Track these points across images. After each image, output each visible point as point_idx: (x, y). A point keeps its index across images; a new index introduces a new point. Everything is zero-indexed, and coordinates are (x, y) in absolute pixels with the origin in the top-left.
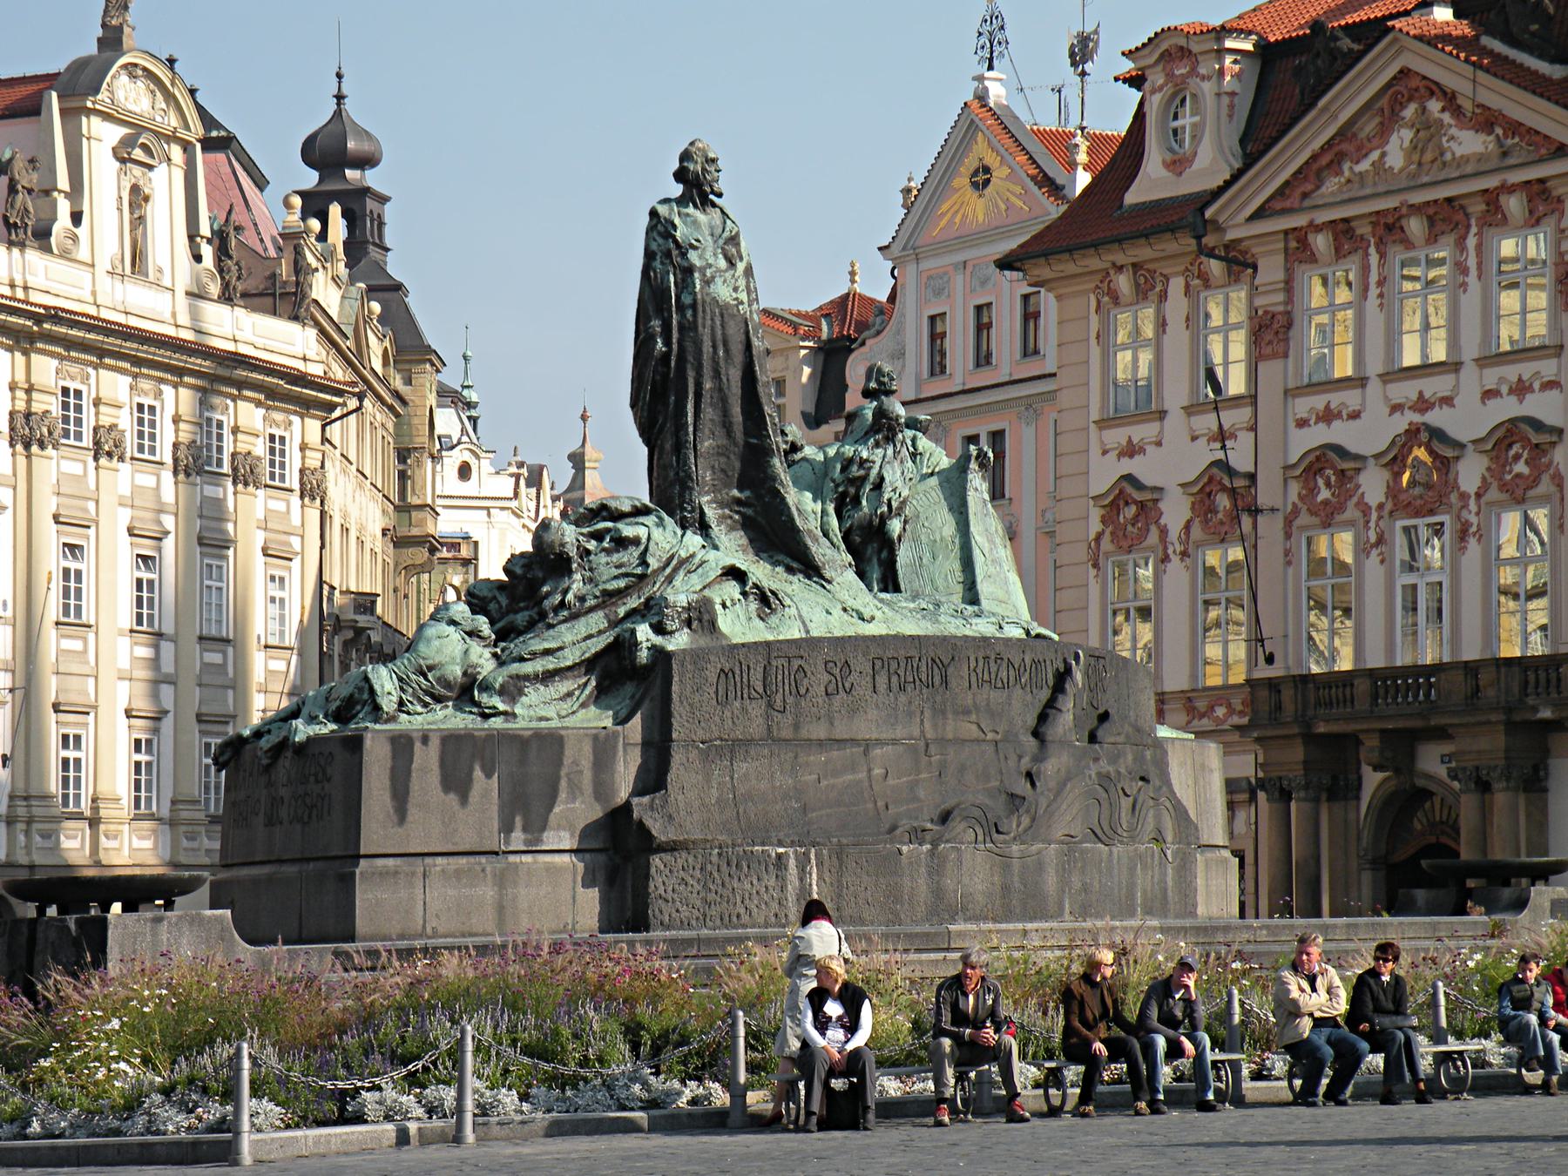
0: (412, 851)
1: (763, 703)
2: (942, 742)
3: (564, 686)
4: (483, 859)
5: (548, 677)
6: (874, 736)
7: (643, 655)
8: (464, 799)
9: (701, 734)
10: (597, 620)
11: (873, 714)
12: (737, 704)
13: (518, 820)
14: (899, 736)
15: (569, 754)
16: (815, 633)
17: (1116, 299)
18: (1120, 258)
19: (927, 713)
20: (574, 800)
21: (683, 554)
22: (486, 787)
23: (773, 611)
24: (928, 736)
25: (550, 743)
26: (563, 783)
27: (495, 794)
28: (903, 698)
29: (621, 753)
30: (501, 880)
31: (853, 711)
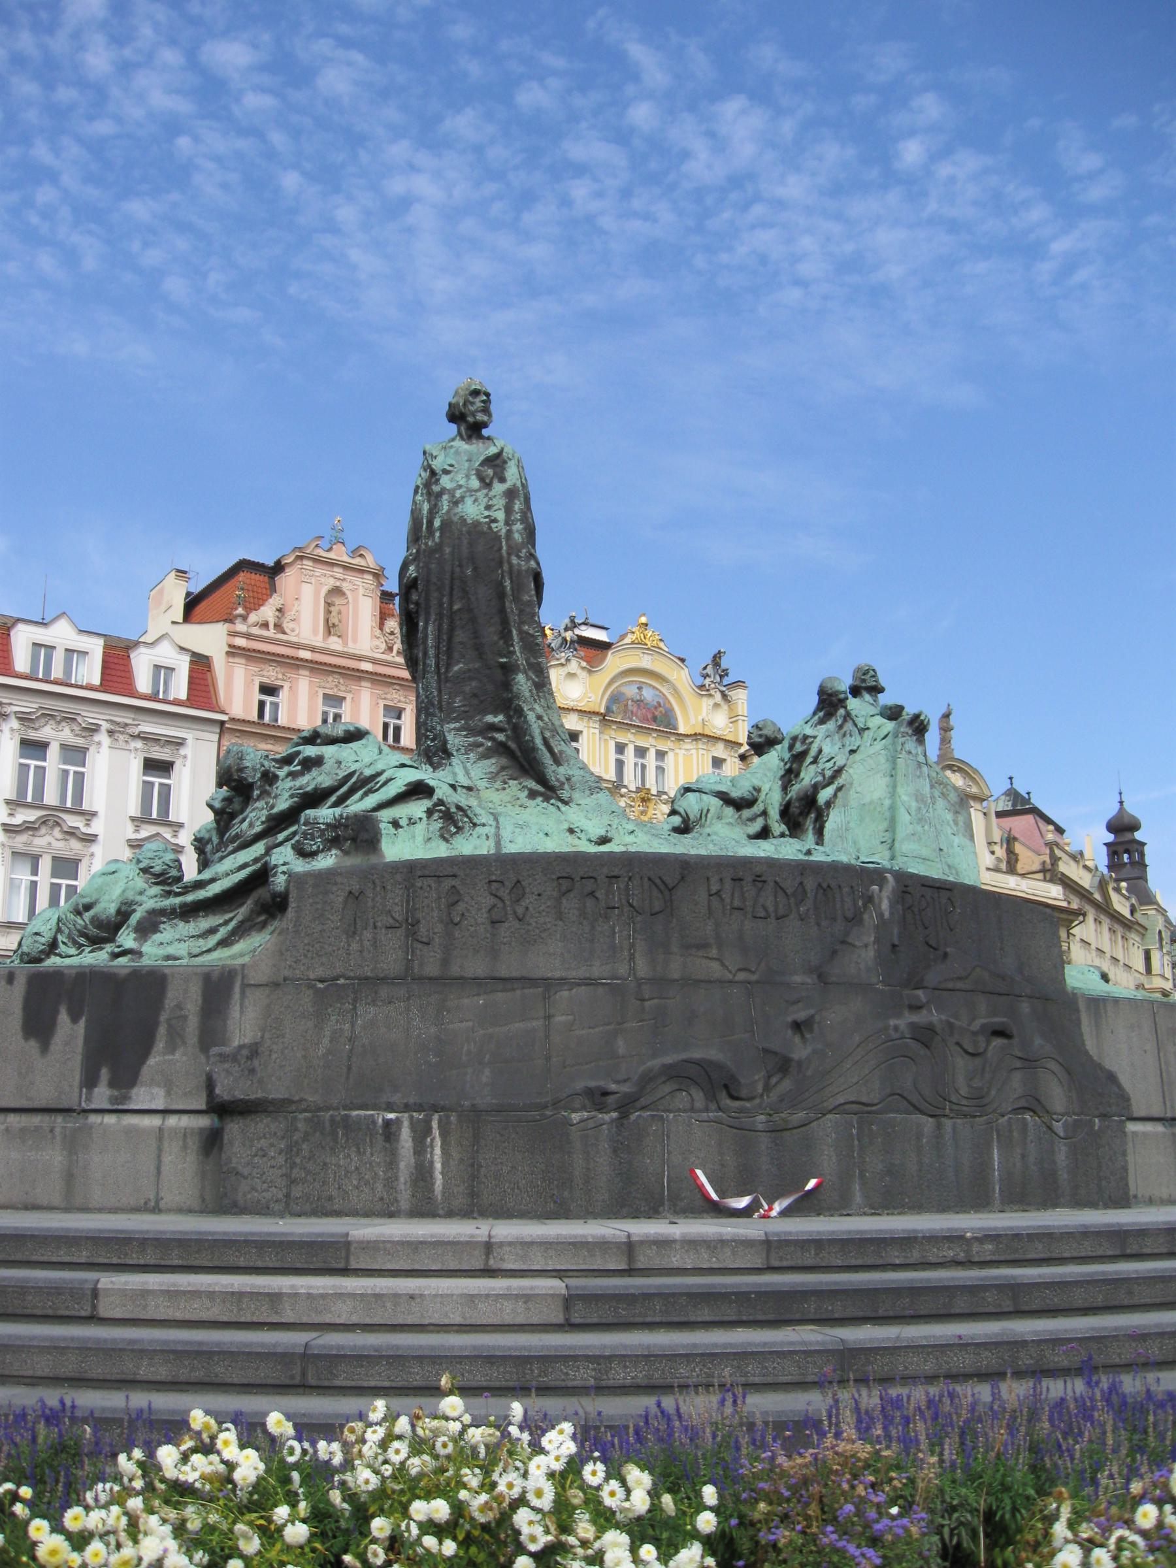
1: (401, 932)
3: (205, 923)
4: (59, 1119)
5: (189, 912)
6: (557, 974)
7: (279, 881)
8: (45, 1047)
9: (320, 972)
10: (259, 848)
12: (368, 934)
13: (105, 1073)
14: (596, 974)
15: (172, 996)
16: (504, 851)
19: (641, 946)
20: (173, 1052)
21: (368, 772)
22: (70, 1033)
23: (459, 829)
25: (151, 984)
26: (162, 1030)
27: (80, 1041)
29: (237, 996)
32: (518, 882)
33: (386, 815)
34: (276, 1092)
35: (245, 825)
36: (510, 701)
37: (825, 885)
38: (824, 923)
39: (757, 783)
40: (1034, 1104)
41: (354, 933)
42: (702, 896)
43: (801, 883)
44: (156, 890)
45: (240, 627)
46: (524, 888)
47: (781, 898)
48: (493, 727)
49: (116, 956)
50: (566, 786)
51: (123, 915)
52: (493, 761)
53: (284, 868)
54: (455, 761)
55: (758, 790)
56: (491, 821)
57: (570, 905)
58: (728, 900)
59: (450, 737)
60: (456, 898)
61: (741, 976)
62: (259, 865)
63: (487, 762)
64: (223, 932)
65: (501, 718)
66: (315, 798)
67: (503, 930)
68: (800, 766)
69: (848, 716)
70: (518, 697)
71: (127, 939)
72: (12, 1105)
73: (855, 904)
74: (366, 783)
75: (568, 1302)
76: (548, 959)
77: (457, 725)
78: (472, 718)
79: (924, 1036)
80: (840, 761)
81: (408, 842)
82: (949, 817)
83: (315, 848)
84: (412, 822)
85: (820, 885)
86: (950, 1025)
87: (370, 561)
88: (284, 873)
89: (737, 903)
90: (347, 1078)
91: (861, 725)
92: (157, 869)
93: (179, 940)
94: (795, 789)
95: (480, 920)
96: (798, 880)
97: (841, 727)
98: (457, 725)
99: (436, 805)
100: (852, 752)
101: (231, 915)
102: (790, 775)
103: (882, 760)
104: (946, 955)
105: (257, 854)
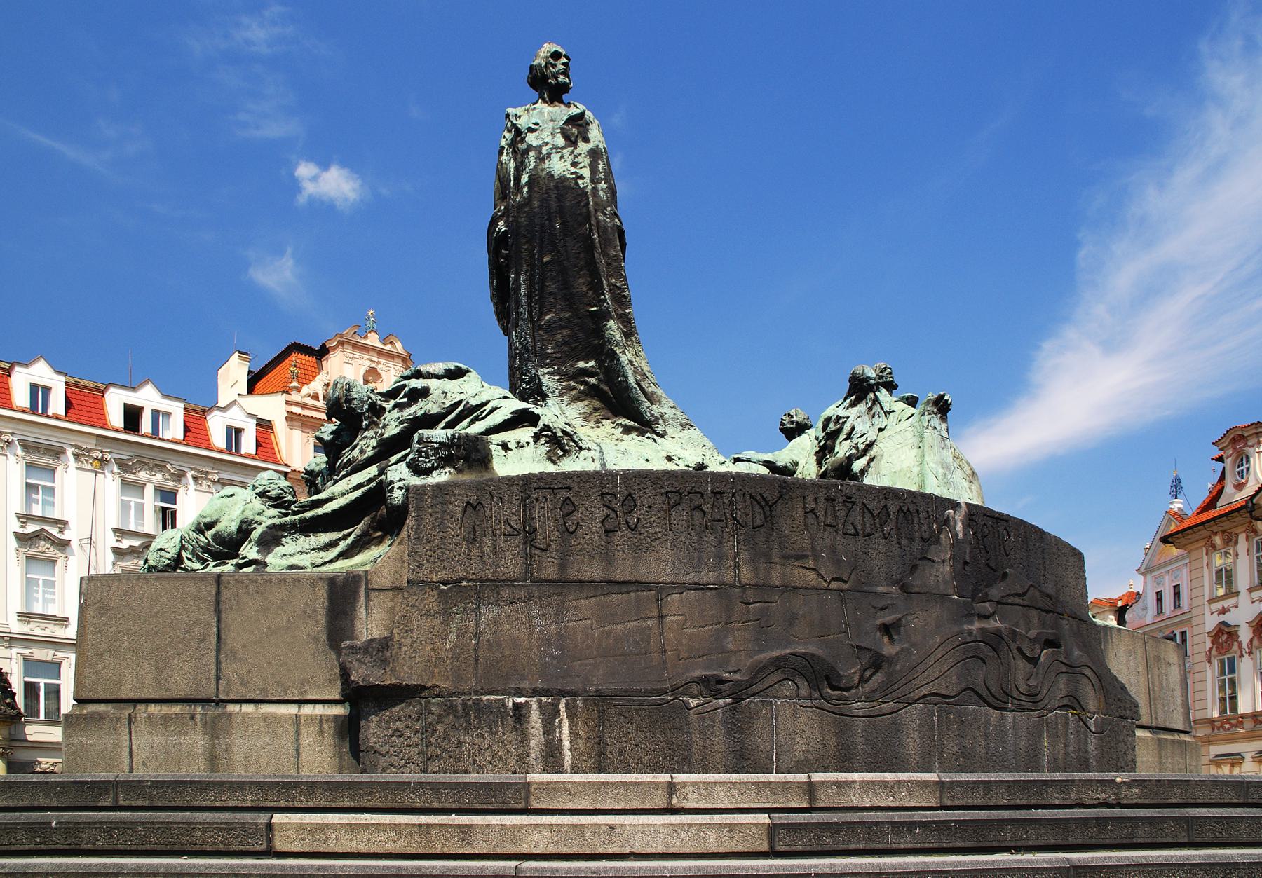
0: (124, 697)
2: (763, 587)
3: (325, 538)
5: (309, 528)
6: (668, 579)
7: (397, 496)
10: (373, 471)
11: (666, 553)
12: (487, 541)
17: (1214, 547)
18: (1215, 529)
19: (744, 554)
21: (474, 402)
24: (745, 580)
28: (709, 538)
30: (214, 729)
31: (640, 549)
32: (630, 494)
33: (496, 438)
34: (410, 678)
35: (356, 452)
36: (602, 346)
37: (905, 509)
38: (905, 542)
39: (796, 459)
40: (1074, 703)
41: (474, 540)
42: (801, 512)
43: (885, 506)
44: (274, 512)
45: (295, 397)
46: (635, 501)
47: (868, 516)
48: (585, 372)
49: (239, 566)
50: (661, 421)
51: (245, 530)
52: (586, 403)
53: (401, 484)
54: (550, 402)
55: (796, 464)
56: (594, 446)
57: (679, 516)
58: (821, 518)
59: (544, 380)
60: (571, 508)
61: (834, 585)
62: (374, 484)
63: (581, 404)
64: (342, 545)
65: (592, 363)
66: (430, 421)
67: (616, 538)
68: (834, 442)
69: (876, 400)
70: (610, 341)
71: (250, 551)
72: (152, 696)
73: (930, 527)
74: (472, 412)
75: (772, 830)
76: (660, 565)
77: (550, 370)
78: (564, 363)
79: (994, 640)
80: (871, 436)
81: (519, 459)
82: (966, 484)
83: (429, 465)
84: (520, 446)
85: (900, 508)
86: (1014, 634)
87: (399, 348)
88: (400, 488)
89: (830, 520)
90: (476, 669)
91: (886, 409)
92: (273, 493)
93: (302, 552)
94: (830, 461)
95: (594, 530)
96: (882, 504)
97: (870, 409)
98: (550, 370)
99: (542, 430)
100: (881, 430)
101: (345, 532)
102: (824, 451)
103: (909, 435)
104: (1005, 575)
105: (372, 476)
